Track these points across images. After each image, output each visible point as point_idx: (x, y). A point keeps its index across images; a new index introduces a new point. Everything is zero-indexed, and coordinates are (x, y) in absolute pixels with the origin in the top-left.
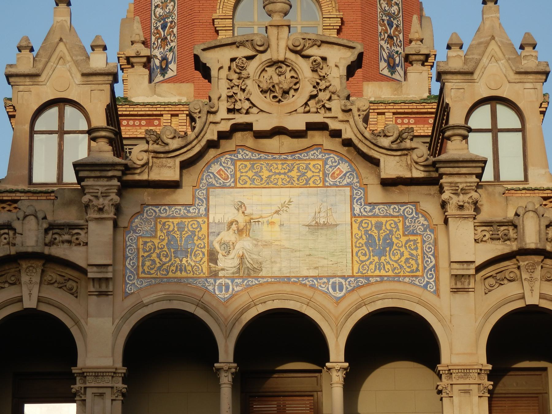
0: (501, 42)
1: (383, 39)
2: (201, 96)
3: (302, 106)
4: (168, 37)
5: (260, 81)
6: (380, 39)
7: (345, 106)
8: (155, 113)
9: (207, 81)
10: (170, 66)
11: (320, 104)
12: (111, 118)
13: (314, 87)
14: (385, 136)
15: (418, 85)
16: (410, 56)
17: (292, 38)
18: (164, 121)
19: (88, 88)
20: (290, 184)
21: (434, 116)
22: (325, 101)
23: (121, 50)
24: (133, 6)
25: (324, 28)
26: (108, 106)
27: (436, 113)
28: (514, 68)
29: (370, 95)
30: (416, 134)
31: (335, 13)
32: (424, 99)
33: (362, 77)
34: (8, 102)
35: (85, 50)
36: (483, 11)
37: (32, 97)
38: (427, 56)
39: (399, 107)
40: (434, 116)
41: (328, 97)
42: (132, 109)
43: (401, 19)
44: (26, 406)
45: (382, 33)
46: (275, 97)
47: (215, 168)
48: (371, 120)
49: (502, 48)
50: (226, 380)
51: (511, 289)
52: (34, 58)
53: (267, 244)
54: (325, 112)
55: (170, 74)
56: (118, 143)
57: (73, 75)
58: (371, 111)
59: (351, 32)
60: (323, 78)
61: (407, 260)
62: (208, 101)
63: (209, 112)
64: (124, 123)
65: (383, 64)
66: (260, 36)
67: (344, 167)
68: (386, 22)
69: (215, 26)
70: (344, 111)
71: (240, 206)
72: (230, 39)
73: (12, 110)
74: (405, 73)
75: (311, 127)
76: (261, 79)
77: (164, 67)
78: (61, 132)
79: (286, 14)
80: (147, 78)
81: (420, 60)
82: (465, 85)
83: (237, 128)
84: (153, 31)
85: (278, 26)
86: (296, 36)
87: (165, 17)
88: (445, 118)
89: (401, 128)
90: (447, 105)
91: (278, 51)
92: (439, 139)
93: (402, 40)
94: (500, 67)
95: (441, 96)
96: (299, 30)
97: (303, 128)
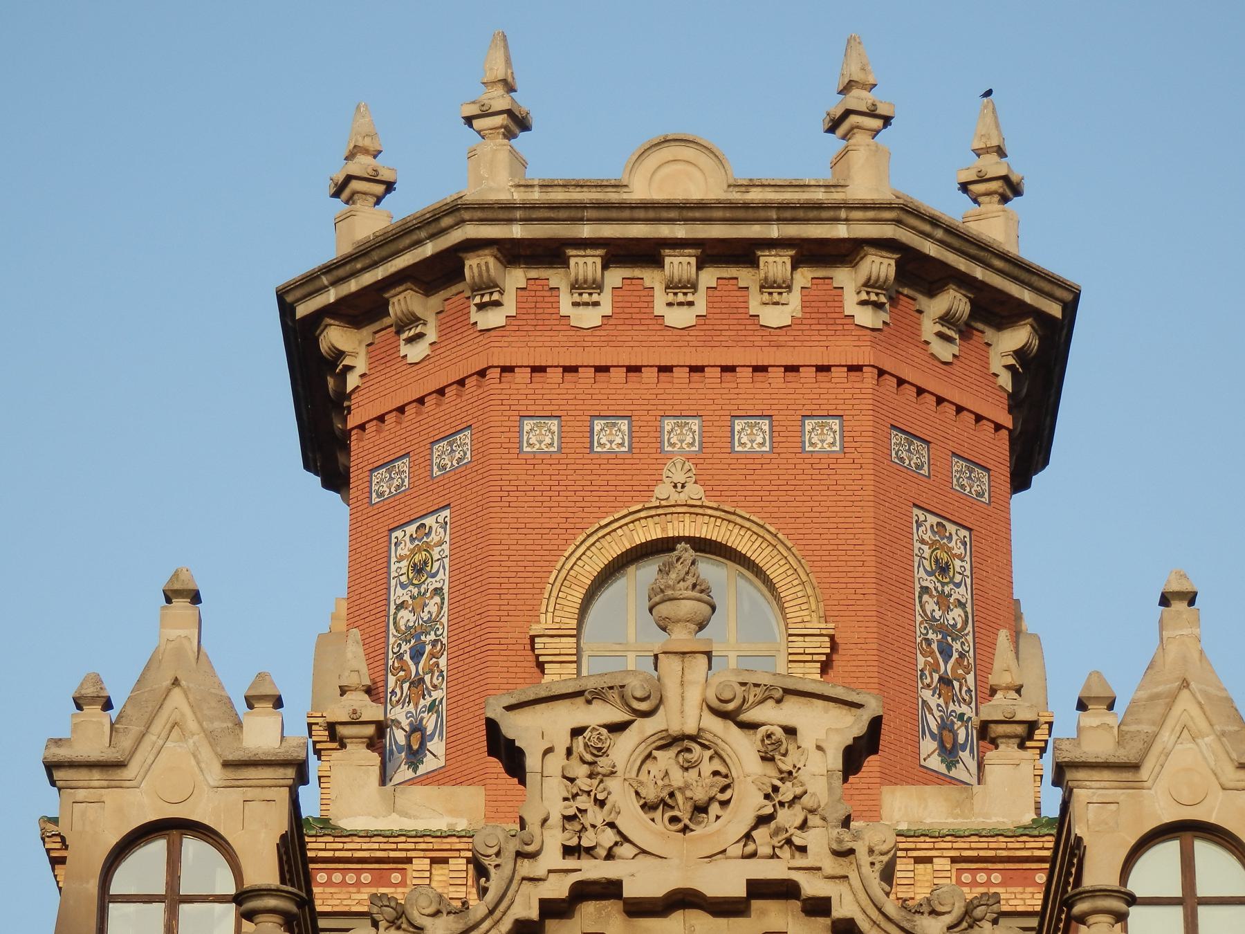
0: (1204, 693)
1: (929, 686)
2: (502, 815)
3: (738, 842)
4: (427, 678)
5: (641, 783)
6: (920, 685)
7: (840, 841)
8: (392, 854)
9: (516, 780)
10: (429, 745)
11: (780, 838)
12: (290, 866)
13: (767, 797)
14: (933, 912)
15: (1012, 792)
16: (992, 725)
17: (715, 681)
18: (415, 874)
19: (236, 795)
21: (1047, 866)
22: (791, 831)
23: (315, 706)
24: (345, 604)
25: (791, 658)
26: (283, 837)
27: (1053, 861)
28: (1234, 756)
29: (897, 816)
30: (1005, 908)
31: (816, 625)
32: (1025, 828)
33: (878, 775)
34: (50, 827)
35: (233, 707)
36: (1161, 621)
37: (106, 815)
38: (1032, 726)
39: (966, 845)
40: (1047, 866)
41: (798, 822)
42: (340, 846)
43: (970, 638)
45: (927, 673)
46: (674, 820)
48: (899, 874)
49: (1207, 708)
52: (112, 725)
54: (793, 857)
55: (429, 764)
57: (203, 765)
58: (899, 854)
59: (854, 669)
60: (788, 776)
62: (517, 827)
63: (519, 854)
64: (321, 877)
65: (928, 746)
66: (641, 677)
68: (934, 646)
69: (537, 652)
70: (837, 854)
72: (571, 683)
73: (58, 846)
74: (980, 766)
75: (759, 890)
76: (643, 776)
77: (415, 747)
78: (173, 899)
79: (701, 626)
80: (375, 772)
81: (1016, 736)
82: (1120, 795)
83: (584, 892)
84: (390, 663)
85: (684, 653)
86: (725, 678)
87: (419, 631)
88: (1073, 870)
89: (970, 894)
90: (1079, 840)
91: (682, 711)
92: (1059, 920)
93: (973, 688)
94: (1201, 752)
96: (733, 663)
97: (741, 892)
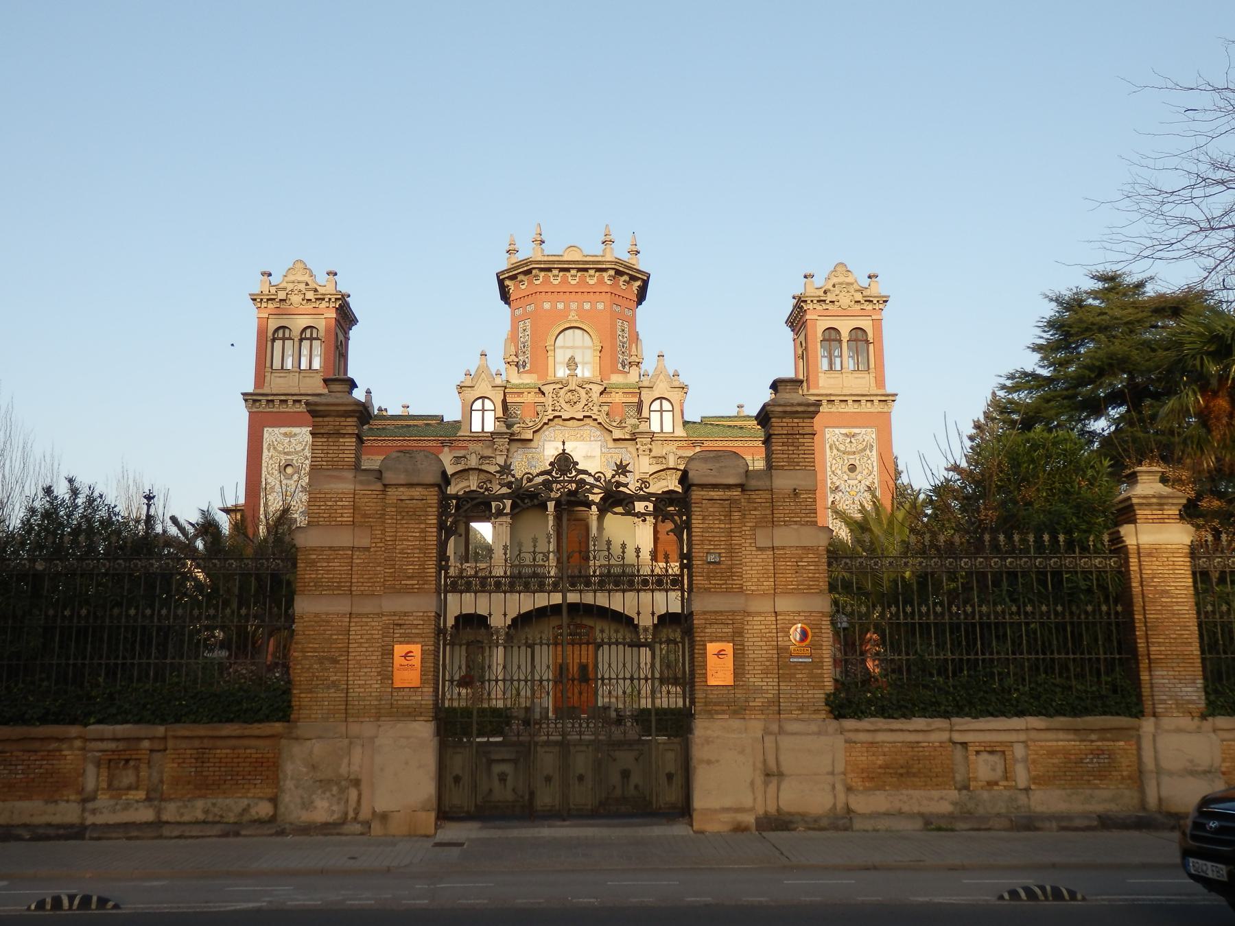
20: (576, 440)
50: (551, 518)
51: (663, 483)
56: (509, 426)
91: (572, 386)
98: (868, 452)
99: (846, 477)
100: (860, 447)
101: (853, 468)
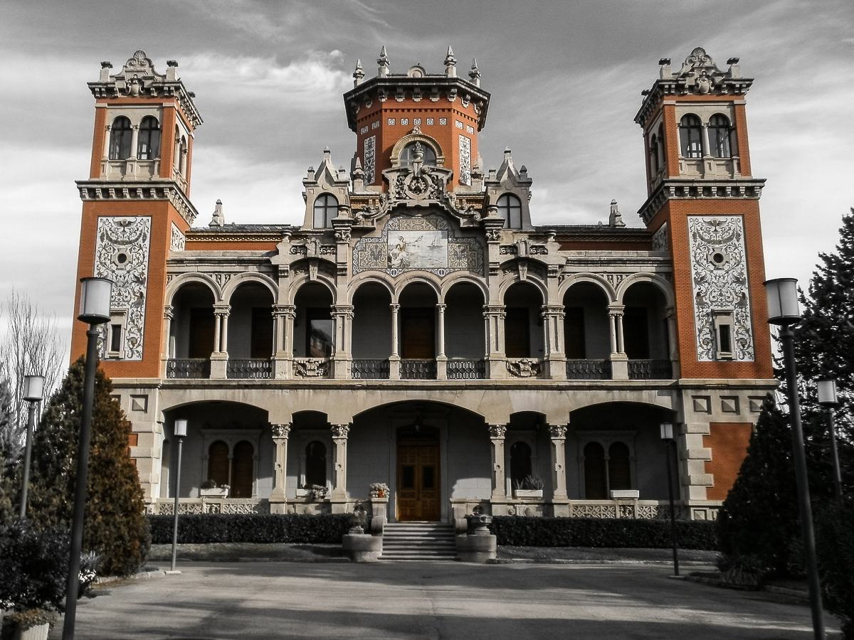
44: (312, 321)
47: (390, 222)
53: (412, 254)
61: (471, 262)
67: (445, 223)
71: (401, 238)
95: (486, 193)
98: (734, 240)
99: (712, 267)
100: (726, 236)
101: (719, 258)
